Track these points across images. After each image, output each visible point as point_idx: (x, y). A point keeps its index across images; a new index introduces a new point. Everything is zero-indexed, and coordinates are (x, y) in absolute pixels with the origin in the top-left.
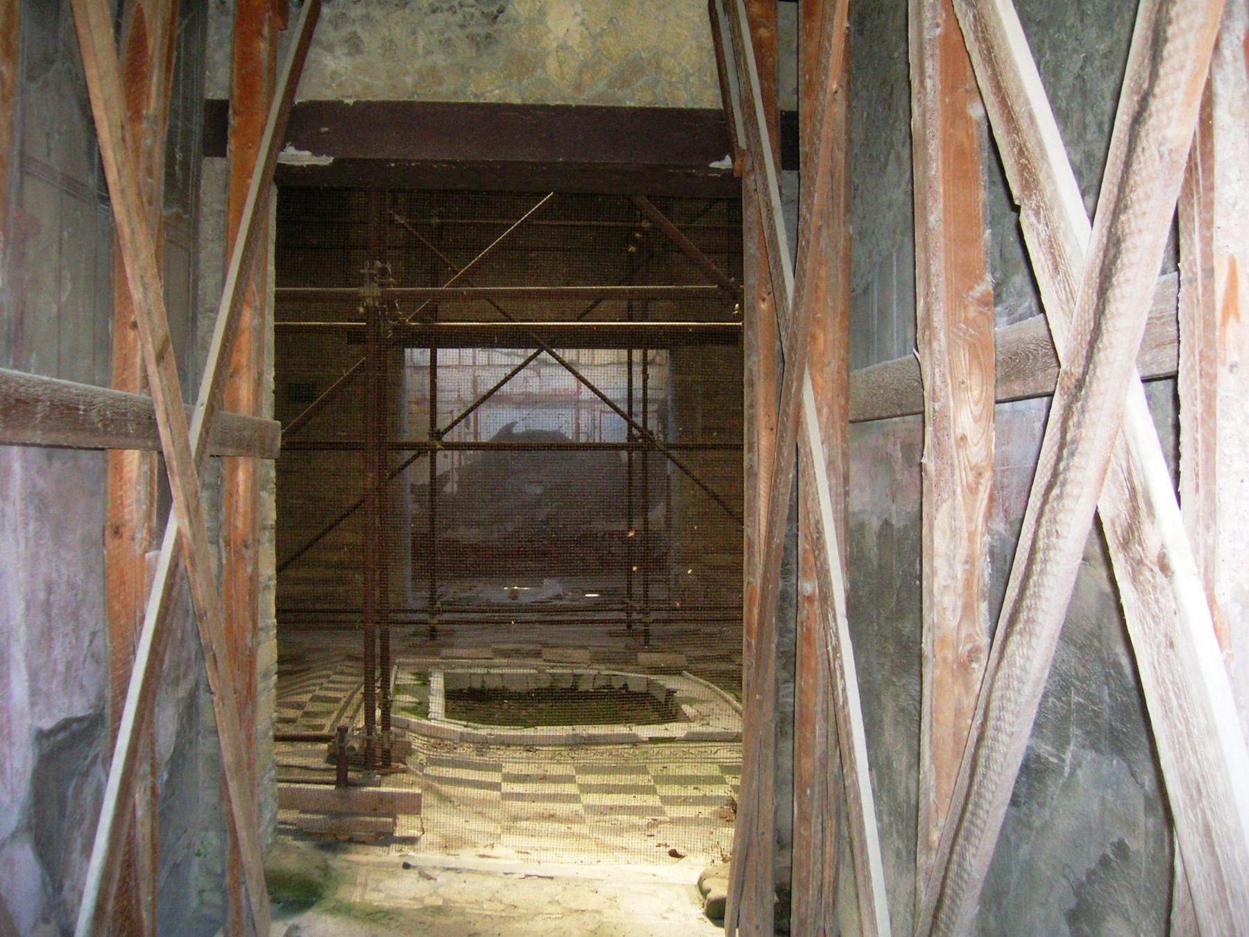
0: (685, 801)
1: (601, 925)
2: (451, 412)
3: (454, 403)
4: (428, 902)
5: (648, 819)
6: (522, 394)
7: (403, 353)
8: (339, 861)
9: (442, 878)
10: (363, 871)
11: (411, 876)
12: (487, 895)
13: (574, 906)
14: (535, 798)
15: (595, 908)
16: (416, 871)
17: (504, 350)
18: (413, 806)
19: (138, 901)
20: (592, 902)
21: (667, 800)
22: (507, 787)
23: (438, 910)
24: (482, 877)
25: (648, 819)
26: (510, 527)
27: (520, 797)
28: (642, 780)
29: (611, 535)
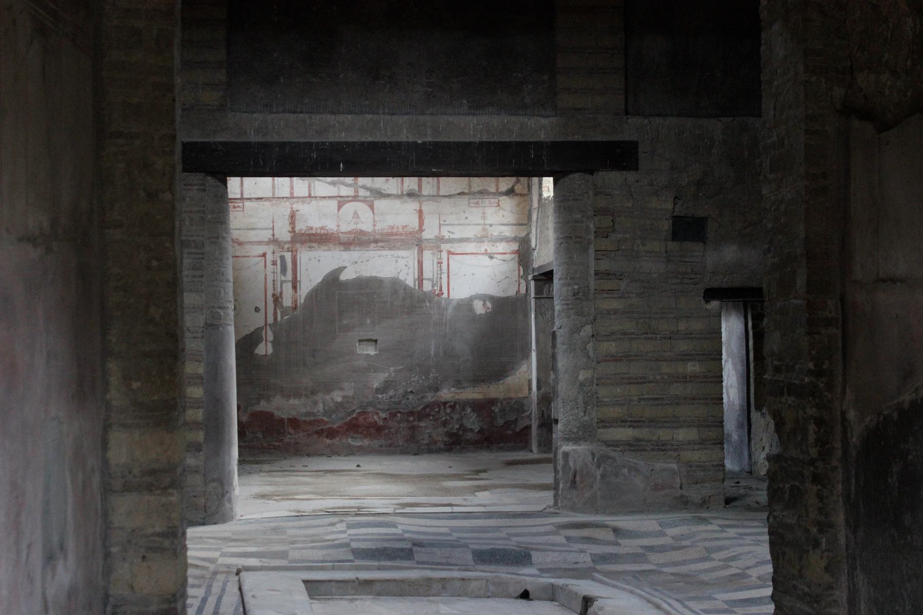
2: (264, 255)
3: (268, 243)
6: (349, 232)
7: (225, 183)
17: (329, 179)
26: (338, 396)
29: (465, 404)
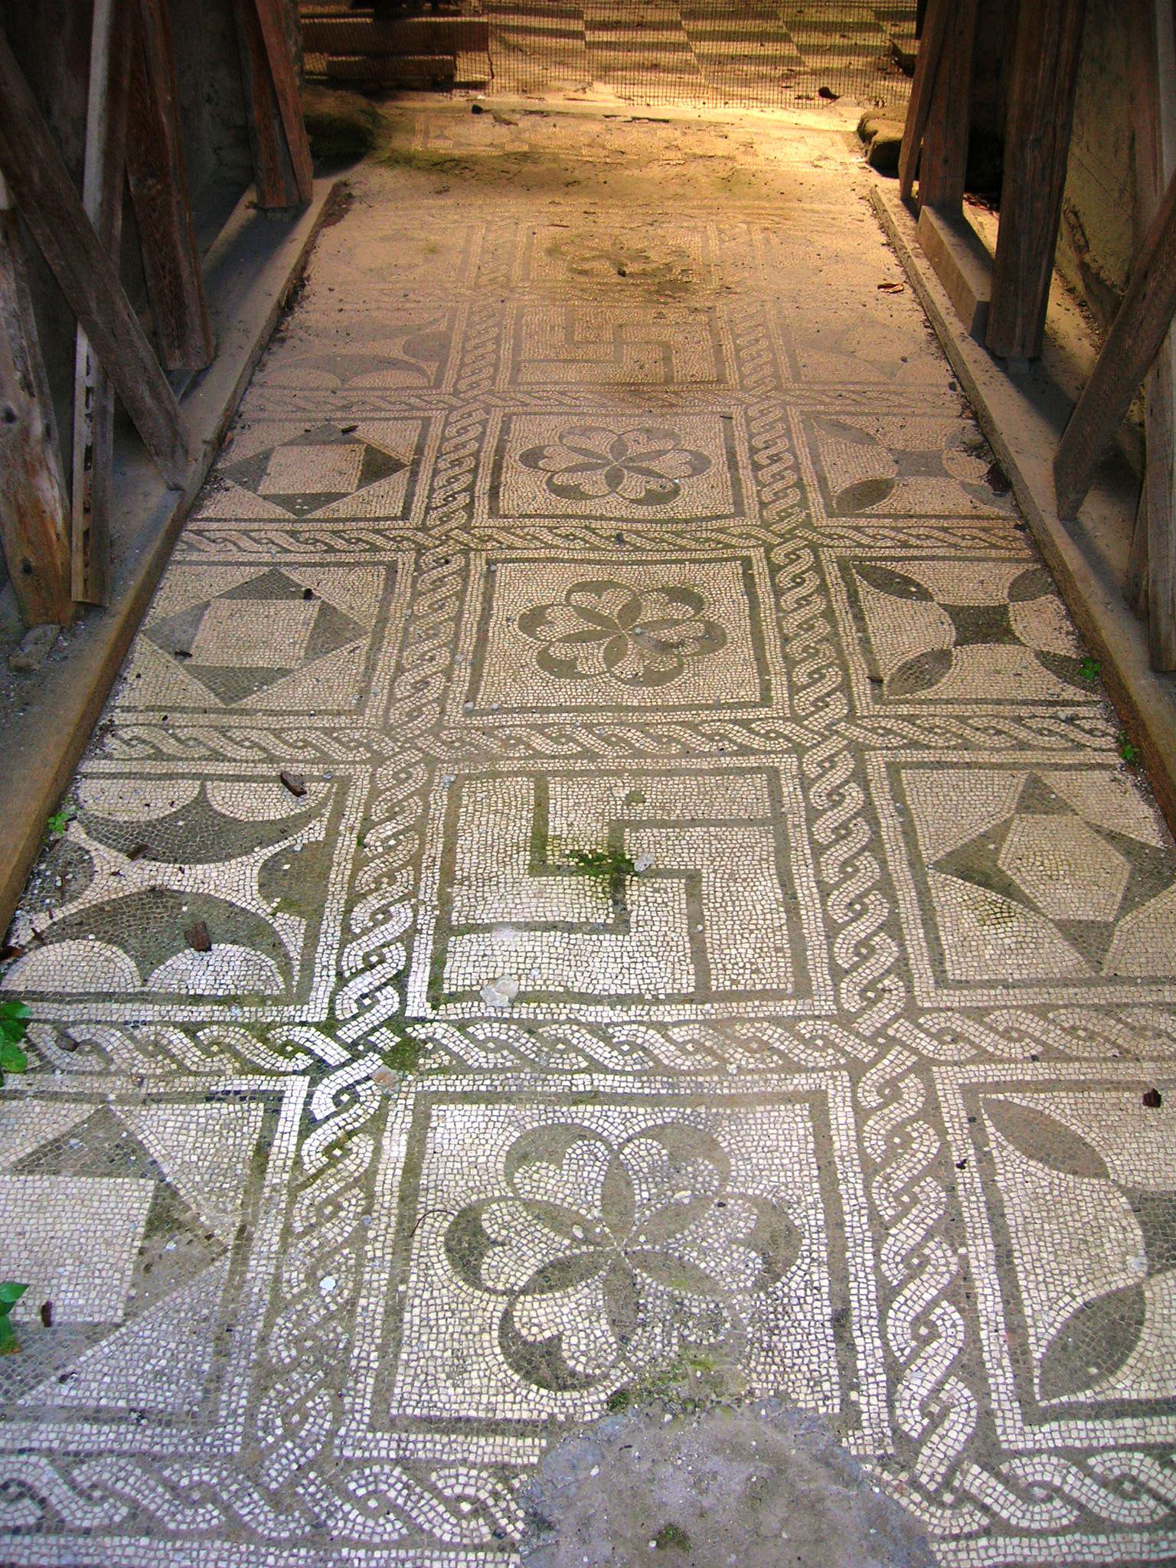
0: (832, 50)
1: (734, 172)
4: (509, 148)
5: (782, 70)
8: (388, 110)
9: (525, 123)
10: (422, 117)
11: (483, 123)
12: (585, 140)
13: (698, 151)
14: (630, 47)
15: (726, 154)
16: (491, 116)
18: (477, 39)
19: (154, 102)
20: (721, 148)
21: (803, 49)
22: (590, 36)
23: (524, 157)
24: (576, 121)
25: (782, 70)
27: (609, 46)
28: (769, 26)
